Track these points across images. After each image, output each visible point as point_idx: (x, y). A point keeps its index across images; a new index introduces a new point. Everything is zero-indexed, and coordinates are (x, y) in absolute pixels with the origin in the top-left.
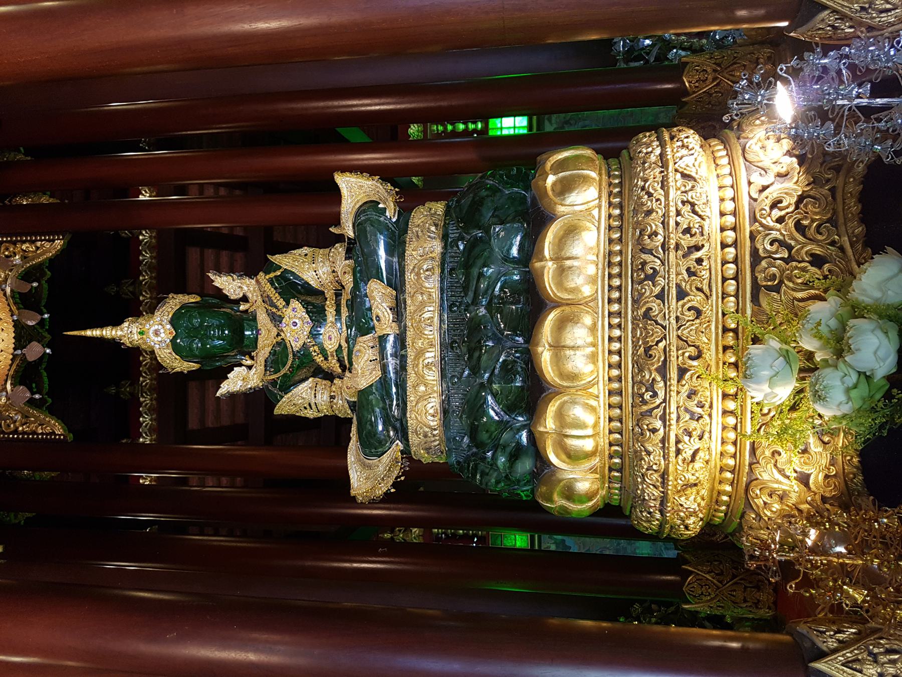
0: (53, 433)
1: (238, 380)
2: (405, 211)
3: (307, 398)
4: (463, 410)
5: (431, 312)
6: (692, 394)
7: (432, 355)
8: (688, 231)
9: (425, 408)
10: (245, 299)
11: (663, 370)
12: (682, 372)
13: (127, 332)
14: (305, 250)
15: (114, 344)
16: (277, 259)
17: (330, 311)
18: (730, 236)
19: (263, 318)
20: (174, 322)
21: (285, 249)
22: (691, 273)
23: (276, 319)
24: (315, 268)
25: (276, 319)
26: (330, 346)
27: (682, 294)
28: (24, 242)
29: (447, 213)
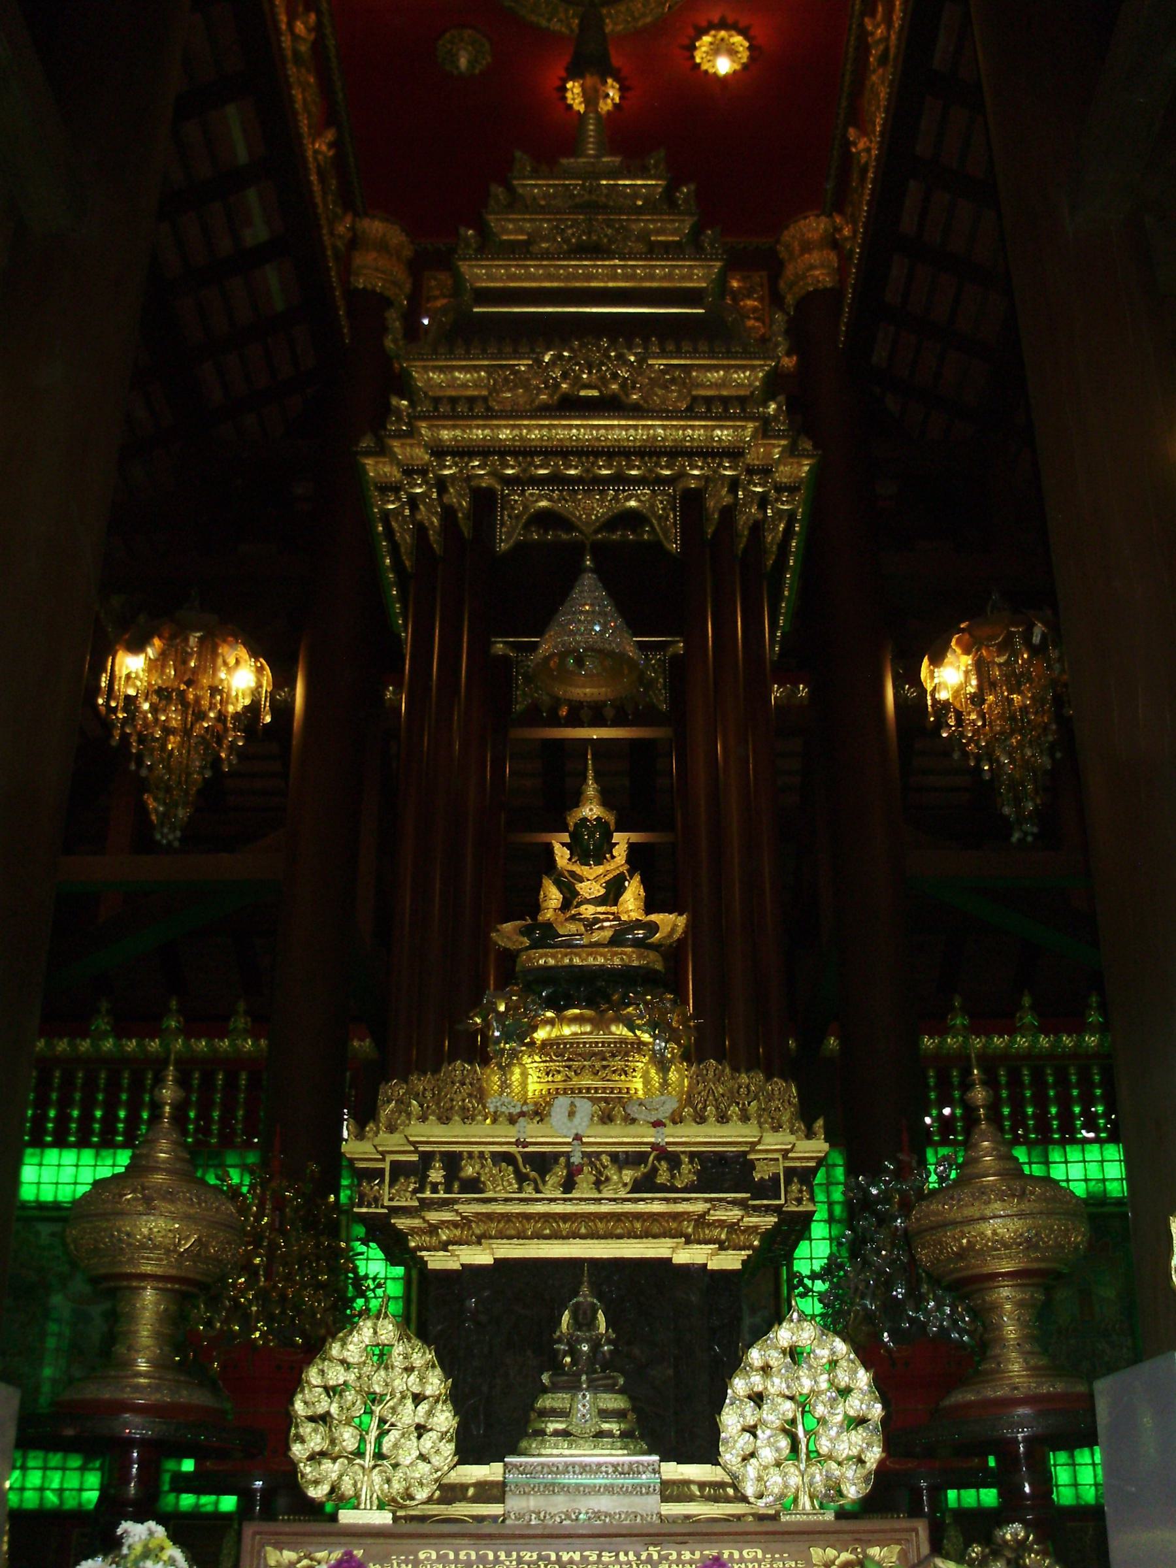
0: (517, 703)
1: (562, 856)
2: (655, 947)
3: (553, 896)
4: (548, 976)
5: (601, 960)
6: (559, 1072)
7: (577, 961)
8: (634, 1070)
9: (545, 959)
10: (613, 857)
11: (569, 1060)
12: (569, 1067)
13: (591, 789)
14: (643, 893)
15: (585, 778)
16: (637, 878)
17: (600, 909)
18: (632, 1092)
19: (600, 870)
20: (598, 819)
21: (643, 881)
22: (614, 1072)
23: (596, 879)
24: (631, 902)
25: (596, 879)
26: (582, 908)
27: (604, 1067)
28: (665, 680)
29: (656, 971)
